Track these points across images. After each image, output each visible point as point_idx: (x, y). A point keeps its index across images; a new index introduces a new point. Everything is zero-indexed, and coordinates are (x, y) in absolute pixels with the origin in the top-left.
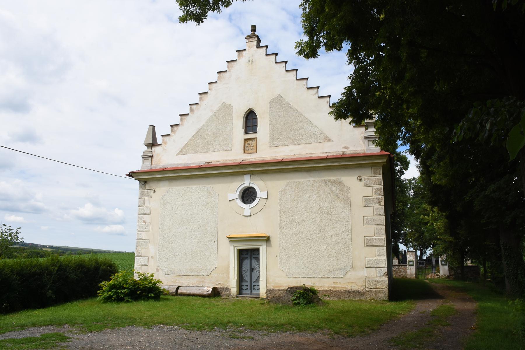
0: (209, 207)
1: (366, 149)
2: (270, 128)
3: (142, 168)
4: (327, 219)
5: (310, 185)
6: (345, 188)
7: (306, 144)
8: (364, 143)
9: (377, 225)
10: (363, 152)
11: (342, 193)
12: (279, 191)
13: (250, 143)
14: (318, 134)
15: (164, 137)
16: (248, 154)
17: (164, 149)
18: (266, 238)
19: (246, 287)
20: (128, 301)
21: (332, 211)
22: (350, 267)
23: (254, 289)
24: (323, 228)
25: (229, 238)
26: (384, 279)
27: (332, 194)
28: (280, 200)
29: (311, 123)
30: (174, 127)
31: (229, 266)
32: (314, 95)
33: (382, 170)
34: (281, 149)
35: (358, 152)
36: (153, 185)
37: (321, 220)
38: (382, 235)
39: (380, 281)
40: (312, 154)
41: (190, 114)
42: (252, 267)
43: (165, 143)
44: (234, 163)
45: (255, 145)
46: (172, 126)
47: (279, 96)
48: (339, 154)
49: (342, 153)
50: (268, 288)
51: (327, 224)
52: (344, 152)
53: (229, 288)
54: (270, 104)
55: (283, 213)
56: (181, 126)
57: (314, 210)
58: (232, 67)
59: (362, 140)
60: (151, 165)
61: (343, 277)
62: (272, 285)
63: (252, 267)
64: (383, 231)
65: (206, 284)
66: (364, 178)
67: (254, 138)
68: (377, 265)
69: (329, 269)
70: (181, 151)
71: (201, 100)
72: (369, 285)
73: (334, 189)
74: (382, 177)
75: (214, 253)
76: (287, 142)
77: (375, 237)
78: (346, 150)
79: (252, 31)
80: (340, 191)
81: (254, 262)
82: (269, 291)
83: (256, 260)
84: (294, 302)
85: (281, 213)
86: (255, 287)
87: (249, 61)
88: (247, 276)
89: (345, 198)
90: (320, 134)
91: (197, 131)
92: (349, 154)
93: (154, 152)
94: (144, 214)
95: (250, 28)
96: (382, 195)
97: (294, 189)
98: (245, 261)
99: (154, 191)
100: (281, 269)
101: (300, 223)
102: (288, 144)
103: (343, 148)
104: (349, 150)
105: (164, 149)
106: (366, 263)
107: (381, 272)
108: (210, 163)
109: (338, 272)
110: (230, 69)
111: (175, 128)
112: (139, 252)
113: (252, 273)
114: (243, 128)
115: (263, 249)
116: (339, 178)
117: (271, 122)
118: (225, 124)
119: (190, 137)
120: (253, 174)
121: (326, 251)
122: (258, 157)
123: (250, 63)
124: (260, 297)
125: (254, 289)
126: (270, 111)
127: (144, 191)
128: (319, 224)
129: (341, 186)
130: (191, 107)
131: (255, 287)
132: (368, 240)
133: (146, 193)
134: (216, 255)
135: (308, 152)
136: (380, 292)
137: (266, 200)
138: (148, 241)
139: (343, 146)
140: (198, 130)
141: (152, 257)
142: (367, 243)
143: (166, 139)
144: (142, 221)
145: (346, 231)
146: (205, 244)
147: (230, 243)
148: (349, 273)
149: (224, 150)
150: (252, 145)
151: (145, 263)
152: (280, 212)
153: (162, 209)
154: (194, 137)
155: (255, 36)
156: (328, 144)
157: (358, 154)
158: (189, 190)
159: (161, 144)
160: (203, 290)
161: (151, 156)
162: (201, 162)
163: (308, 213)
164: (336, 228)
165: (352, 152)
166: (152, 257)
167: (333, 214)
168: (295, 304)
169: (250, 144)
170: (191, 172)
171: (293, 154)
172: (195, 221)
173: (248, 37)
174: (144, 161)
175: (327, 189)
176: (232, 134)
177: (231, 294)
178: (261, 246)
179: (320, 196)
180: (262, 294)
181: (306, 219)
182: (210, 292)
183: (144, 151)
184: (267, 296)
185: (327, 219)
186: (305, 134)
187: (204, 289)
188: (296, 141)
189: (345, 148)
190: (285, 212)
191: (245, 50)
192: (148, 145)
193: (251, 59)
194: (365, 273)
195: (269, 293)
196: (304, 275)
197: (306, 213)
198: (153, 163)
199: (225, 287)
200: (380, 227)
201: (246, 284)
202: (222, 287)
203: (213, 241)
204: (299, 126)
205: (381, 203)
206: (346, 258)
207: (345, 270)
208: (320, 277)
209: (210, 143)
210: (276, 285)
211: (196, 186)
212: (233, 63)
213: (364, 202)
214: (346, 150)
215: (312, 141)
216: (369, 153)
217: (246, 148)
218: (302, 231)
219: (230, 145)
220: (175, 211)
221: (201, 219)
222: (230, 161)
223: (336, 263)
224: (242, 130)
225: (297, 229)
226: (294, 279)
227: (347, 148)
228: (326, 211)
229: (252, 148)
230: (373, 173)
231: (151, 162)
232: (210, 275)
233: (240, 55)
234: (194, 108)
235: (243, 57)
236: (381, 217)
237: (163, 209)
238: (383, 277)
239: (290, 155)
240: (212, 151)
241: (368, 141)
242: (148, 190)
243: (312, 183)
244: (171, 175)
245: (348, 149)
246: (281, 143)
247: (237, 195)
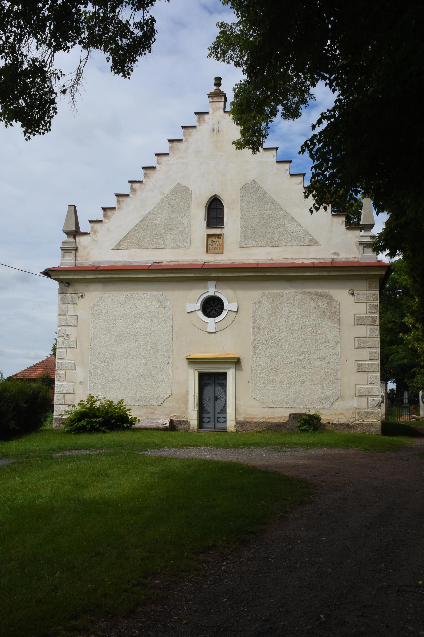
0: (161, 319)
1: (360, 257)
2: (241, 223)
3: (61, 264)
4: (312, 339)
5: (291, 297)
6: (334, 303)
7: (286, 246)
8: (358, 249)
9: (370, 348)
10: (356, 260)
11: (329, 308)
12: (252, 303)
13: (215, 240)
14: (302, 234)
15: (93, 223)
16: (212, 254)
17: (94, 240)
18: (236, 360)
19: (208, 420)
20: (104, 432)
21: (317, 330)
22: (337, 397)
23: (218, 421)
24: (306, 350)
25: (187, 359)
26: (377, 411)
27: (318, 309)
28: (254, 314)
29: (293, 219)
30: (107, 210)
31: (187, 394)
32: (298, 184)
33: (378, 283)
34: (254, 250)
35: (351, 260)
36: (80, 288)
37: (303, 340)
38: (376, 360)
39: (373, 413)
40: (294, 259)
41: (131, 195)
42: (216, 395)
43: (95, 232)
44: (194, 265)
45: (221, 243)
46: (104, 209)
47: (254, 182)
48: (327, 262)
49: (331, 260)
50: (237, 421)
51: (311, 345)
52: (333, 259)
53: (187, 421)
54: (242, 192)
55: (257, 330)
56: (118, 210)
57: (296, 327)
58: (190, 135)
59: (356, 246)
60: (75, 261)
61: (328, 407)
62: (243, 416)
63: (216, 395)
64: (377, 355)
65: (157, 416)
66: (357, 292)
67: (220, 235)
68: (370, 394)
69: (312, 398)
70: (119, 245)
71: (146, 177)
72: (359, 417)
73: (320, 303)
74: (378, 292)
75: (168, 377)
76: (263, 243)
77: (367, 362)
78: (336, 257)
79: (215, 85)
80: (327, 306)
81: (219, 390)
82: (239, 424)
83: (221, 386)
84: (300, 428)
85: (254, 331)
86: (219, 420)
87: (214, 130)
88: (209, 406)
89: (333, 315)
90: (304, 234)
91: (142, 219)
92: (340, 262)
93: (79, 243)
94: (67, 326)
95: (213, 82)
96: (377, 313)
97: (271, 302)
98: (206, 388)
99: (82, 296)
100: (254, 397)
101: (278, 343)
102: (264, 245)
103: (332, 254)
104: (339, 257)
105: (94, 240)
106: (357, 392)
107: (374, 402)
108: (160, 262)
109: (323, 401)
110: (187, 137)
111: (109, 213)
112: (62, 376)
113: (216, 402)
114: (205, 220)
115: (231, 374)
116: (327, 290)
117: (242, 215)
118: (181, 214)
119: (131, 226)
120: (219, 281)
121: (309, 377)
122: (225, 259)
123: (215, 132)
124: (227, 431)
125: (218, 421)
126: (241, 200)
127: (66, 295)
128: (301, 344)
129: (329, 300)
130: (132, 186)
131: (219, 420)
132: (359, 365)
133: (70, 298)
134: (171, 380)
136: (371, 425)
137: (236, 313)
138: (74, 361)
139: (333, 251)
140: (143, 218)
141: (80, 382)
142: (358, 369)
143: (96, 227)
144: (65, 336)
145: (333, 354)
146: (156, 366)
147: (189, 366)
148: (337, 403)
149: (179, 247)
150: (217, 243)
151: (71, 390)
152: (254, 329)
153: (93, 319)
155: (221, 95)
156: (313, 248)
157: (350, 262)
158: (132, 297)
159: (89, 233)
160: (157, 422)
161: (76, 248)
162: (147, 261)
163: (289, 331)
164: (322, 350)
165: (343, 260)
167: (319, 332)
168: (302, 431)
169: (214, 242)
170: (137, 274)
171: (270, 258)
172: (142, 337)
173: (212, 95)
174: (64, 254)
175: (311, 303)
176: (190, 226)
177: (191, 428)
178: (229, 369)
179: (303, 312)
180: (230, 427)
181: (285, 339)
182: (168, 425)
183: (63, 241)
184: (236, 430)
185: (312, 339)
187: (159, 421)
188: (274, 242)
189: (335, 254)
190: (259, 329)
191: (207, 113)
192: (68, 233)
193: (216, 127)
194: (355, 403)
195: (239, 426)
196: (282, 405)
197: (286, 332)
198: (78, 258)
199: (182, 419)
200: (373, 350)
201: (208, 415)
202: (178, 419)
203: (167, 362)
204: (278, 223)
205: (376, 322)
206: (333, 385)
207: (331, 400)
208: (302, 407)
209: (160, 236)
210: (248, 417)
211: (142, 292)
212: (190, 130)
213: (356, 321)
214: (336, 257)
215: (295, 243)
216: (364, 262)
217: (209, 247)
218: (280, 352)
219: (188, 241)
220: (113, 323)
221: (149, 334)
222: (189, 262)
223: (320, 391)
224: (204, 223)
225: (274, 349)
226: (270, 410)
227: (338, 255)
228: (310, 329)
229: (217, 247)
230: (368, 287)
231: (76, 257)
232: (162, 405)
233: (201, 119)
234: (137, 187)
235: (205, 122)
236: (375, 339)
237: (95, 321)
238: (376, 408)
239: (266, 258)
240: (163, 247)
241: (364, 247)
242: (73, 295)
243: (293, 296)
244: (107, 276)
245: (338, 256)
246: (255, 243)
247: (198, 306)
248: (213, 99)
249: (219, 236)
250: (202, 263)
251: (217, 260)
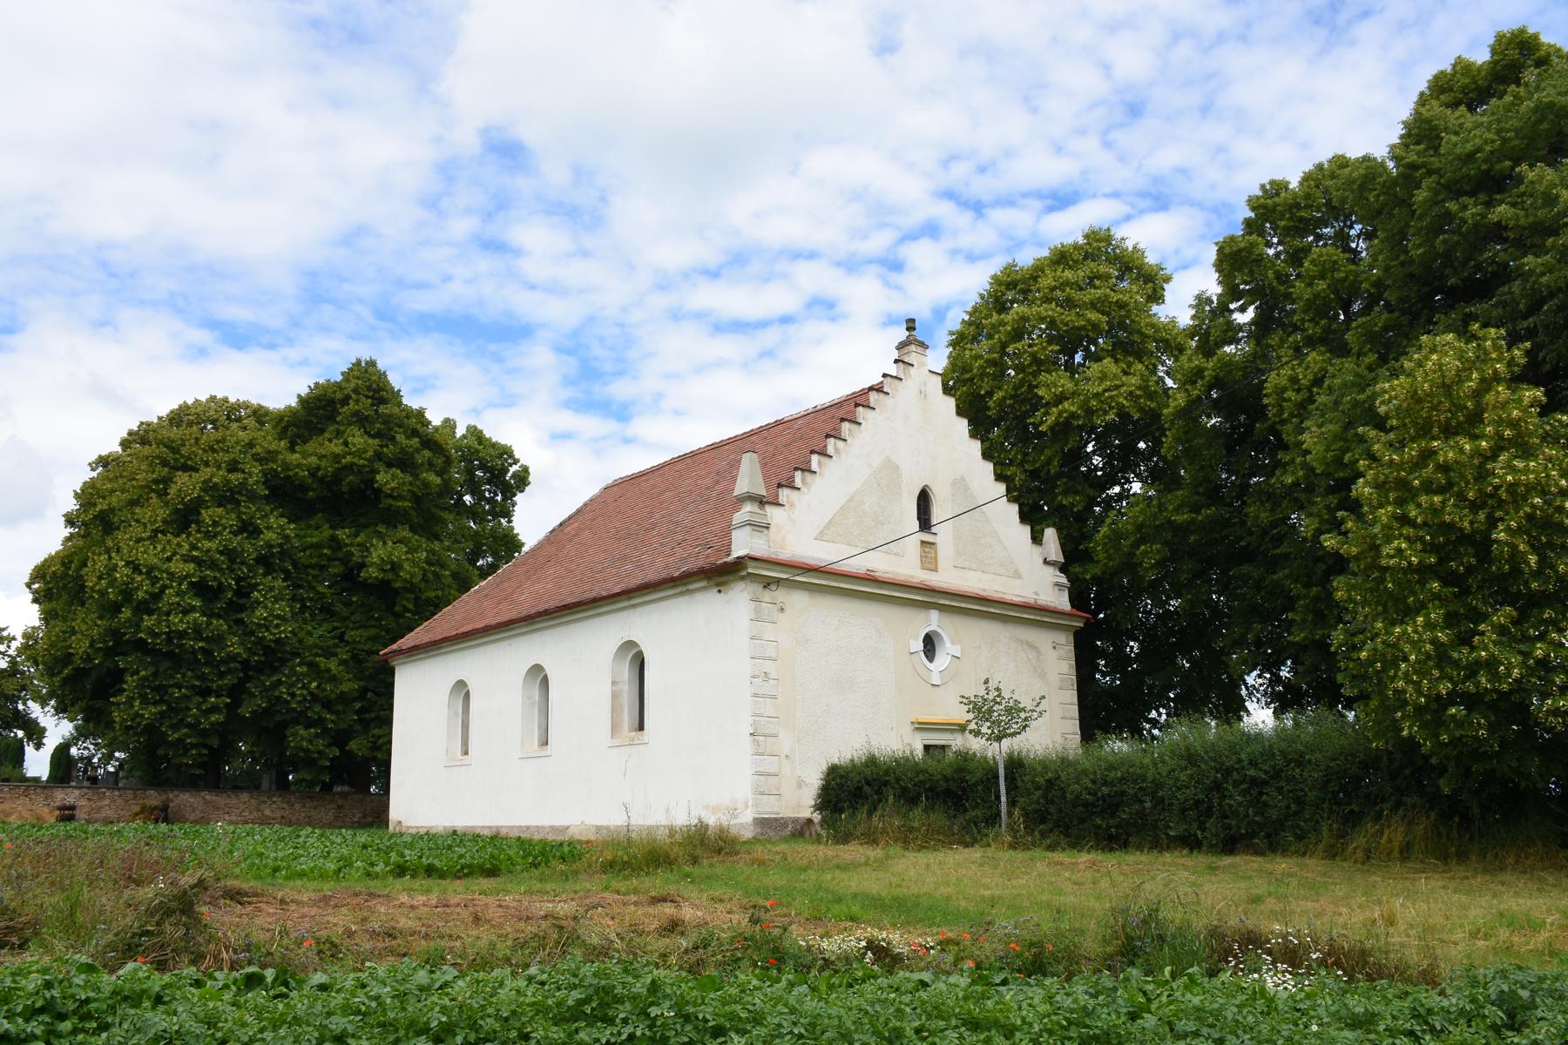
7: (996, 574)
10: (1053, 605)
36: (781, 595)
67: (933, 544)
94: (764, 659)
135: (997, 587)
141: (787, 756)
154: (844, 510)
156: (1018, 582)
166: (787, 756)
227: (1038, 595)
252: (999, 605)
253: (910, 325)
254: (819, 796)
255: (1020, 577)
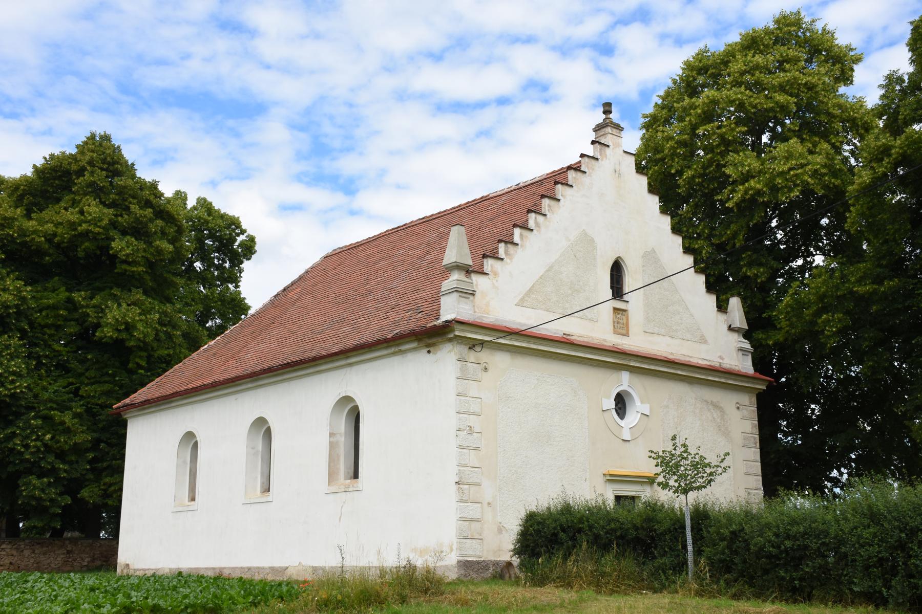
8: (737, 355)
10: (737, 368)
29: (687, 309)
34: (656, 338)
35: (734, 367)
36: (485, 356)
40: (691, 357)
44: (603, 345)
45: (625, 322)
47: (653, 251)
49: (718, 364)
67: (625, 311)
70: (522, 299)
73: (715, 416)
76: (663, 330)
78: (721, 361)
87: (615, 171)
94: (470, 413)
112: (465, 491)
126: (643, 271)
135: (685, 352)
138: (480, 470)
139: (719, 354)
141: (489, 504)
144: (468, 428)
156: (704, 347)
166: (489, 504)
186: (682, 324)
189: (721, 357)
203: (584, 478)
222: (598, 341)
233: (603, 152)
244: (524, 345)
248: (612, 131)
249: (624, 313)
250: (611, 345)
251: (625, 344)
252: (686, 368)
253: (607, 108)
254: (518, 541)
255: (706, 342)
